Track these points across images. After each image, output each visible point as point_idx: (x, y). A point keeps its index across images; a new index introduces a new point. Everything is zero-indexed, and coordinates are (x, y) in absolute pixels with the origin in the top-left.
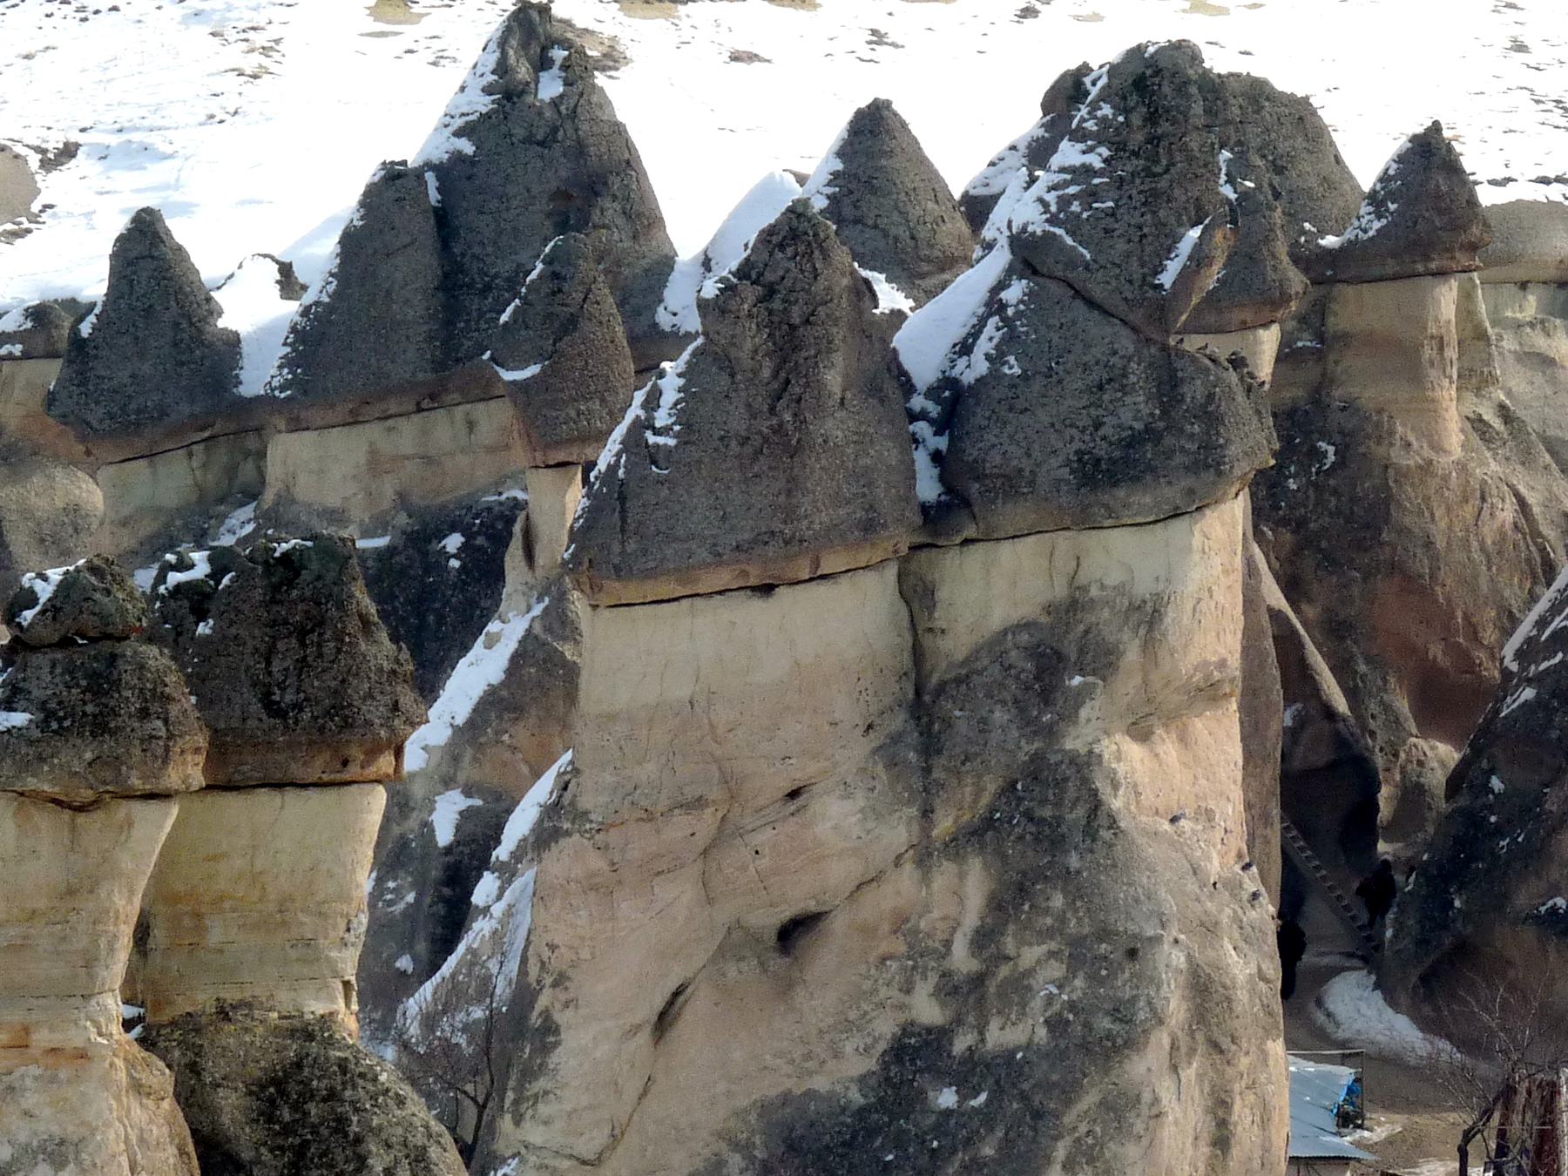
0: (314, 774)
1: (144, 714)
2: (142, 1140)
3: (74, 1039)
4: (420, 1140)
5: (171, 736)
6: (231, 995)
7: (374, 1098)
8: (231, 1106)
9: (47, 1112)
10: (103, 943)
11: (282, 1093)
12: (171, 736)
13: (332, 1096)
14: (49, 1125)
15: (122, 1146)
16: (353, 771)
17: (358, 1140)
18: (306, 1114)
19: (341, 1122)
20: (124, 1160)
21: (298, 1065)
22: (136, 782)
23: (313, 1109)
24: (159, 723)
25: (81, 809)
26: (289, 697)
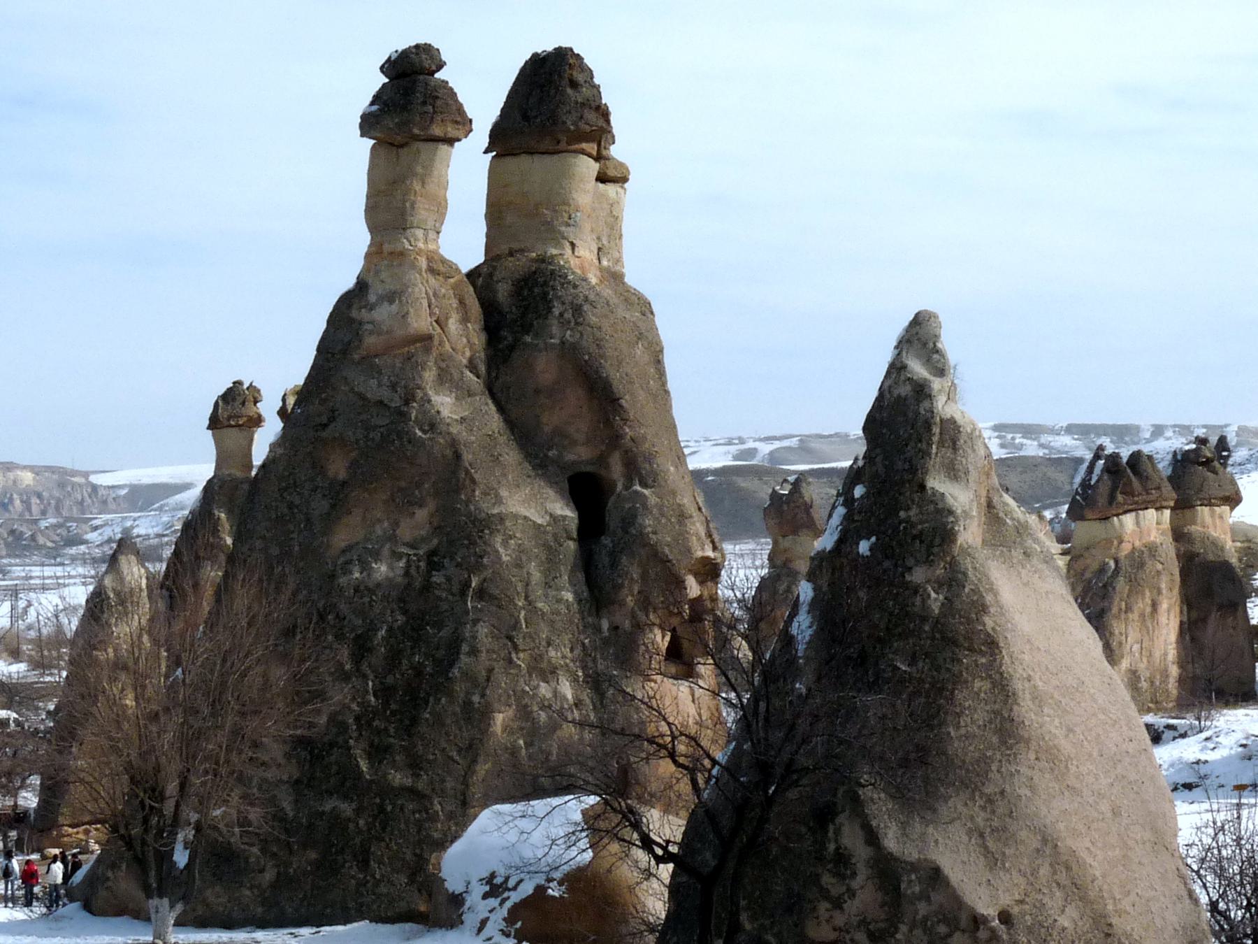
0: (542, 147)
1: (424, 103)
2: (435, 294)
3: (399, 248)
4: (580, 301)
5: (435, 112)
6: (515, 246)
7: (563, 284)
8: (503, 291)
9: (389, 280)
10: (408, 205)
11: (526, 284)
12: (435, 112)
13: (545, 283)
14: (390, 286)
15: (424, 295)
16: (563, 146)
17: (551, 301)
18: (533, 292)
19: (545, 294)
20: (425, 304)
21: (535, 273)
22: (416, 131)
23: (536, 290)
24: (431, 107)
25: (401, 146)
26: (534, 114)
